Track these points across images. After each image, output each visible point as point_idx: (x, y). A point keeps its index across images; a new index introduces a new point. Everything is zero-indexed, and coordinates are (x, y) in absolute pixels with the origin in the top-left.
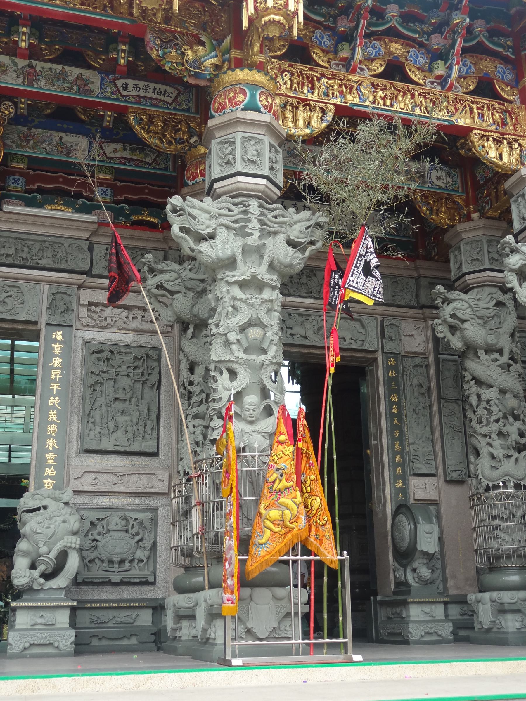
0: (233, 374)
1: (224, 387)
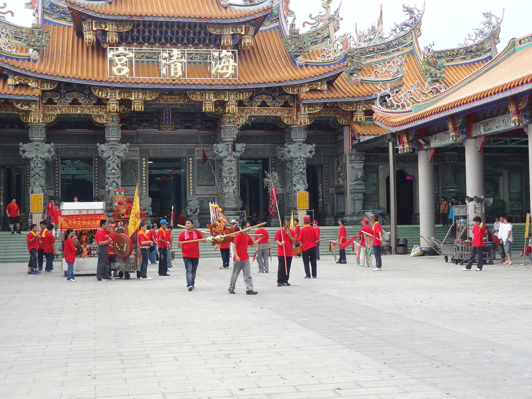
0: (226, 179)
1: (225, 181)
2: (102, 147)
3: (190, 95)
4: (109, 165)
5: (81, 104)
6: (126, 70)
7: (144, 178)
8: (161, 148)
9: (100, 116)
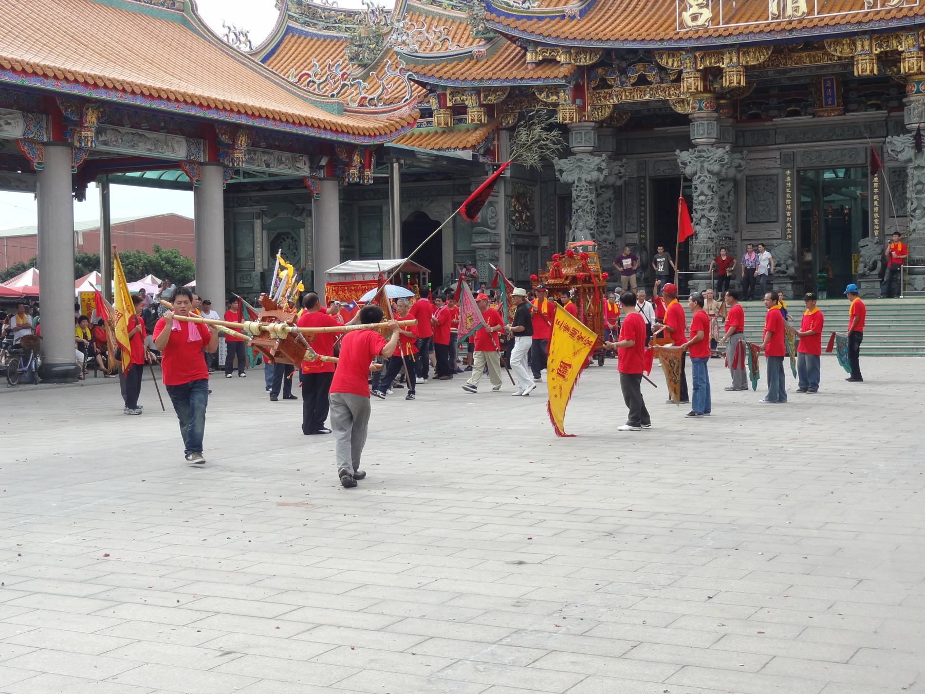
2: (684, 156)
3: (830, 46)
4: (696, 188)
5: (651, 83)
6: (707, 14)
7: (789, 207)
8: (817, 151)
9: (683, 101)
